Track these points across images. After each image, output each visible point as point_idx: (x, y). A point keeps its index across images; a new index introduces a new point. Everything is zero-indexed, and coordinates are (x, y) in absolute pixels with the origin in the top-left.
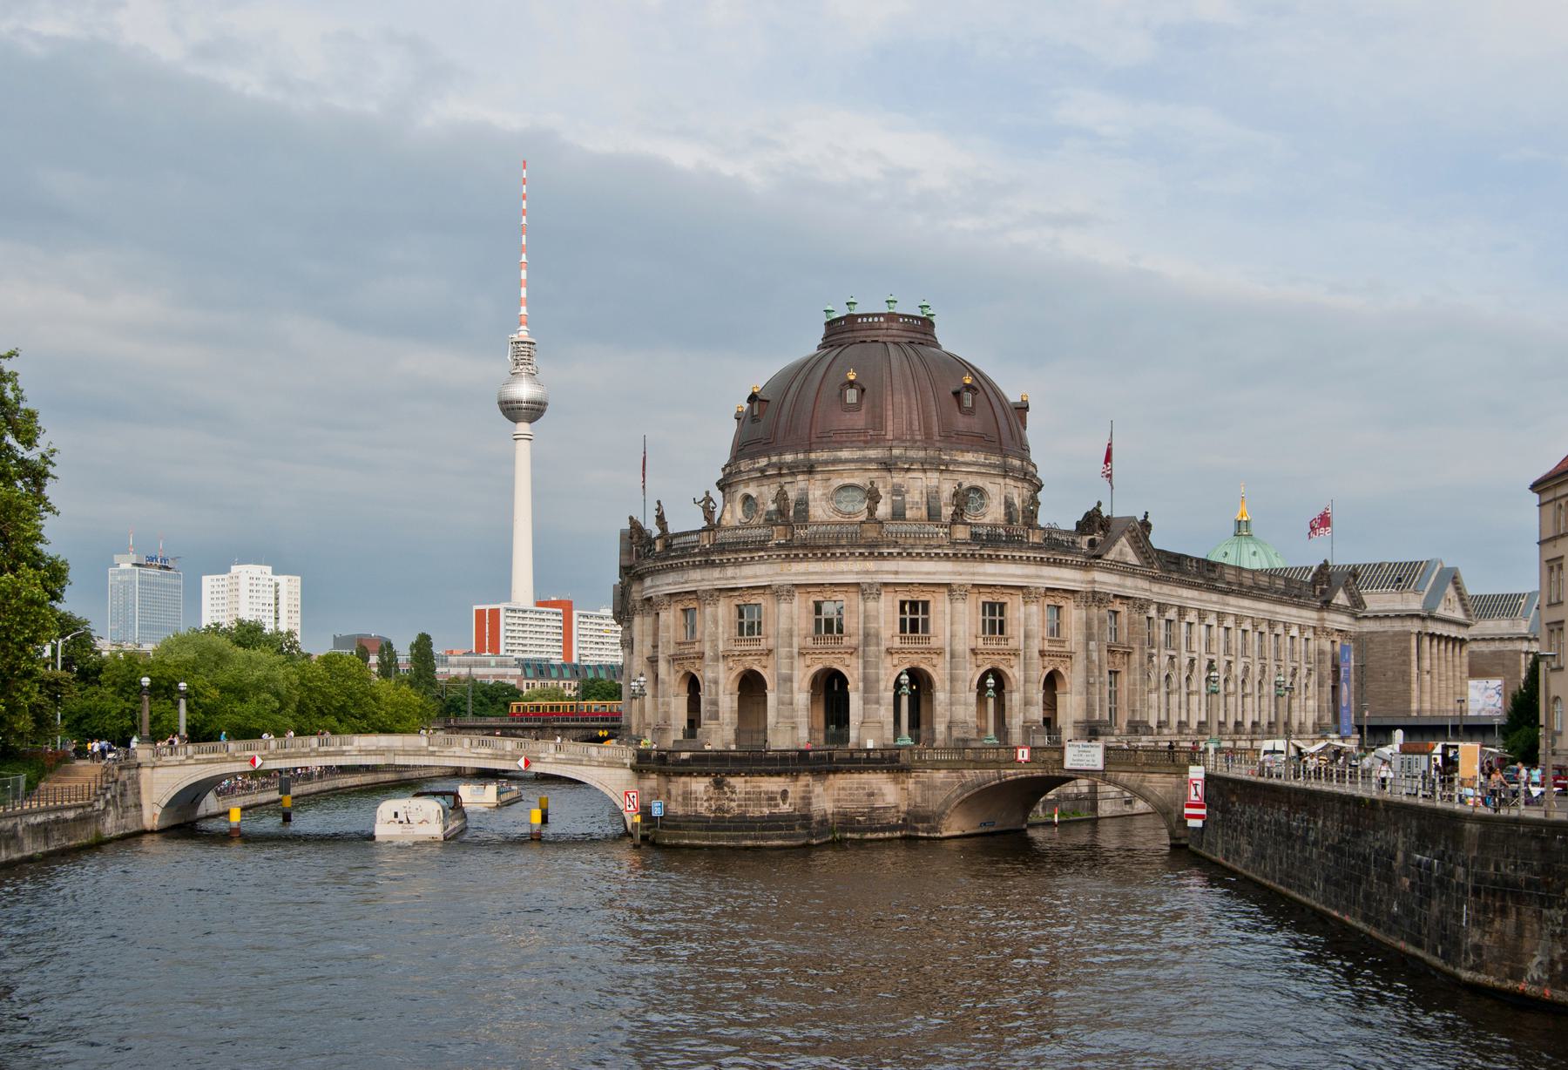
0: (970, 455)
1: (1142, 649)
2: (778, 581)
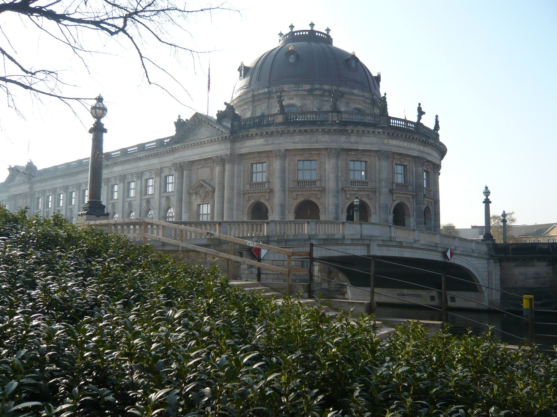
2: (384, 148)
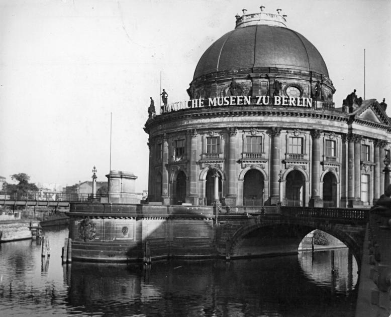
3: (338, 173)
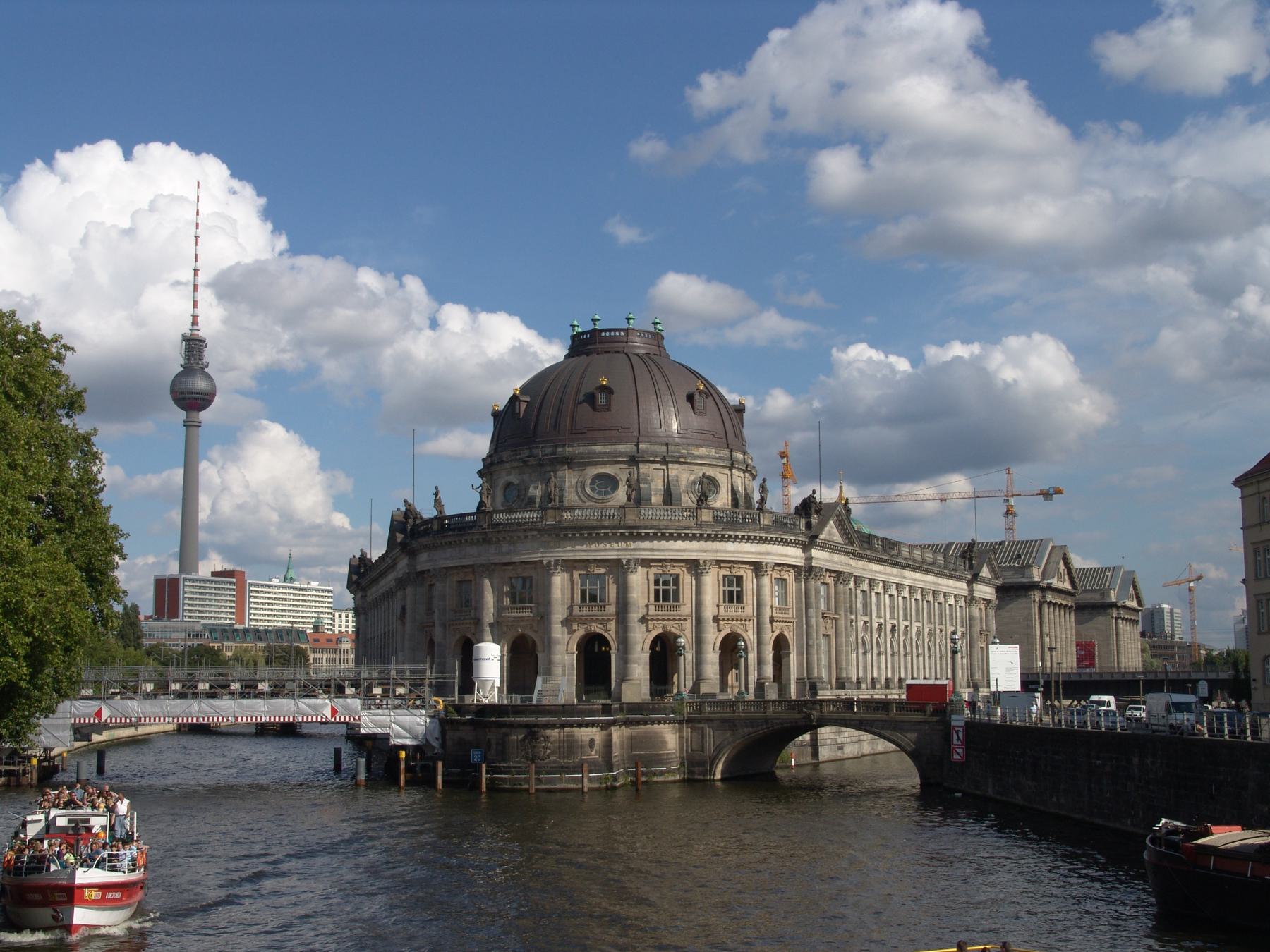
0: (704, 449)
1: (846, 615)
3: (791, 633)
